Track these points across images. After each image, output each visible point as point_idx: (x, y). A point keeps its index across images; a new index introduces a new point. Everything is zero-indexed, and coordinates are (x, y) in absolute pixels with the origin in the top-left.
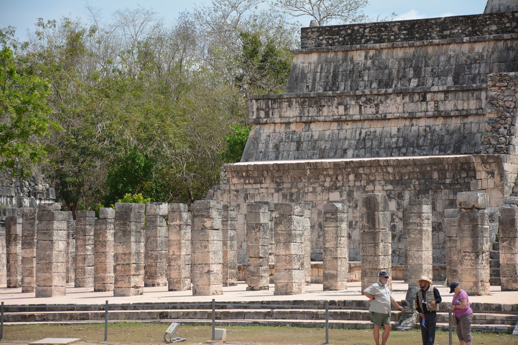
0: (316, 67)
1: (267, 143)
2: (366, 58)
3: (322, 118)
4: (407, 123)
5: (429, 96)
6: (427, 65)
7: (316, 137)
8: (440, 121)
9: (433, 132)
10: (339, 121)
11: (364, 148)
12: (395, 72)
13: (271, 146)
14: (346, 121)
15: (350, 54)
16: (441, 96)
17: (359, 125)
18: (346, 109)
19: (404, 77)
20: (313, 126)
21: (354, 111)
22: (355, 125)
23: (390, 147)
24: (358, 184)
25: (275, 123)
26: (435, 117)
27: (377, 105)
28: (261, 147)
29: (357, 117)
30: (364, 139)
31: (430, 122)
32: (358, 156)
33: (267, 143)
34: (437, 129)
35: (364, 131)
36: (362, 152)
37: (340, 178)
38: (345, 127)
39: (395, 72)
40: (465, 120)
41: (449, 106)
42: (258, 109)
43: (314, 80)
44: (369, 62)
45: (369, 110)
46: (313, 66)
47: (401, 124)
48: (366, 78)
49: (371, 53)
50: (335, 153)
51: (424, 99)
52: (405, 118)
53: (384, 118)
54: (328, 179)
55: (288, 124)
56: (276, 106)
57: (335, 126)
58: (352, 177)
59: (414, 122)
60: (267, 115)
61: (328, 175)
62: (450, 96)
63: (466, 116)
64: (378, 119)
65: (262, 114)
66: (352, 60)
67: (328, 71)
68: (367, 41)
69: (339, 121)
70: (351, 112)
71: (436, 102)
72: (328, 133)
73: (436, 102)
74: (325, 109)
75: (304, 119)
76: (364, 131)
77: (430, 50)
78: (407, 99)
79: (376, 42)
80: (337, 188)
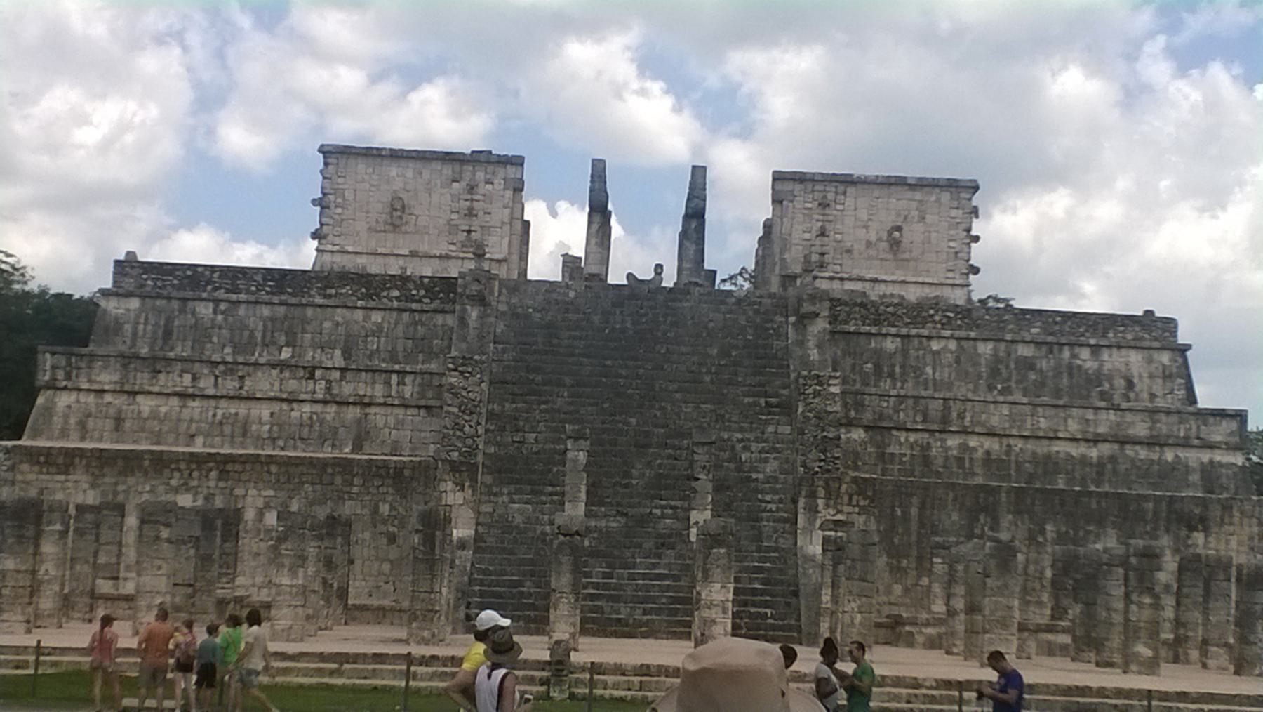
0: (138, 317)
1: (66, 417)
2: (215, 312)
3: (156, 389)
4: (285, 406)
5: (318, 373)
6: (304, 331)
7: (145, 415)
8: (332, 409)
9: (322, 422)
10: (182, 396)
11: (222, 435)
12: (259, 336)
13: (72, 421)
14: (193, 396)
15: (190, 304)
16: (337, 374)
17: (212, 403)
18: (194, 378)
19: (274, 343)
20: (139, 398)
21: (207, 384)
22: (205, 403)
23: (258, 438)
24: (222, 484)
25: (80, 390)
26: (325, 402)
27: (242, 378)
28: (57, 422)
29: (211, 392)
30: (221, 423)
31: (318, 408)
32: (212, 446)
33: (66, 417)
34: (328, 417)
35: (220, 412)
36: (218, 440)
37: (195, 474)
38: (192, 404)
39: (259, 336)
40: (367, 410)
41: (347, 389)
42: (54, 368)
43: (135, 334)
44: (220, 317)
45: (230, 385)
46: (132, 315)
47: (276, 407)
48: (215, 339)
49: (223, 306)
50: (177, 439)
51: (312, 377)
52: (283, 400)
53: (251, 398)
54: (177, 474)
55: (102, 392)
56: (83, 365)
57: (175, 401)
58: (213, 474)
59: (295, 405)
60: (68, 377)
61: (179, 470)
62: (349, 375)
63: (369, 405)
64: (240, 398)
65: (60, 375)
66: (193, 313)
67: (156, 324)
68: (215, 289)
69: (182, 396)
70: (202, 384)
71: (329, 382)
72: (163, 409)
73: (329, 382)
74: (162, 376)
75: (127, 388)
76: (220, 412)
77: (309, 312)
78: (287, 374)
79: (228, 291)
80: (188, 490)
